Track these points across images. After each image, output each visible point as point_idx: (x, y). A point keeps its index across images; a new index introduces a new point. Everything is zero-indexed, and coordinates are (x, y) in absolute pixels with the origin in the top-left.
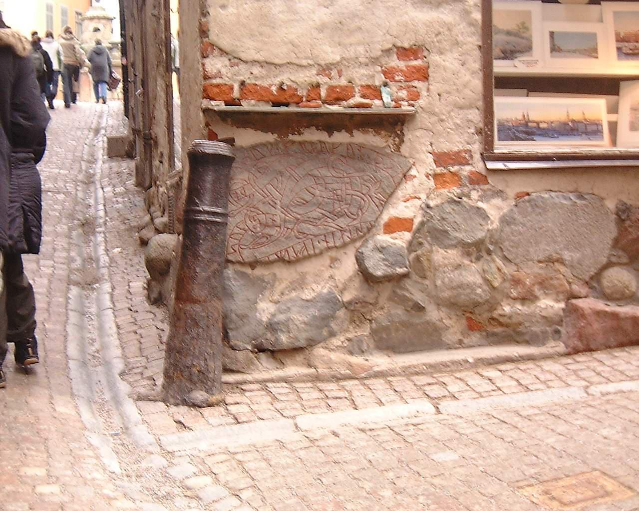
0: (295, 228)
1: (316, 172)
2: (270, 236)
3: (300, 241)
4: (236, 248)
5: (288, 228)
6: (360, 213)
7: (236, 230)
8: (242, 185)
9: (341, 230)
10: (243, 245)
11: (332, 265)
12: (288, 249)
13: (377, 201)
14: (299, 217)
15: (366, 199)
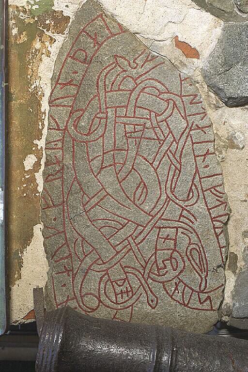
0: (181, 203)
1: (96, 163)
2: (190, 244)
3: (201, 196)
4: (203, 296)
5: (181, 215)
6: (166, 96)
7: (178, 296)
8: (109, 283)
9: (191, 130)
10: (200, 286)
11: (241, 146)
12: (213, 216)
13: (149, 65)
14: (164, 197)
15: (143, 85)
